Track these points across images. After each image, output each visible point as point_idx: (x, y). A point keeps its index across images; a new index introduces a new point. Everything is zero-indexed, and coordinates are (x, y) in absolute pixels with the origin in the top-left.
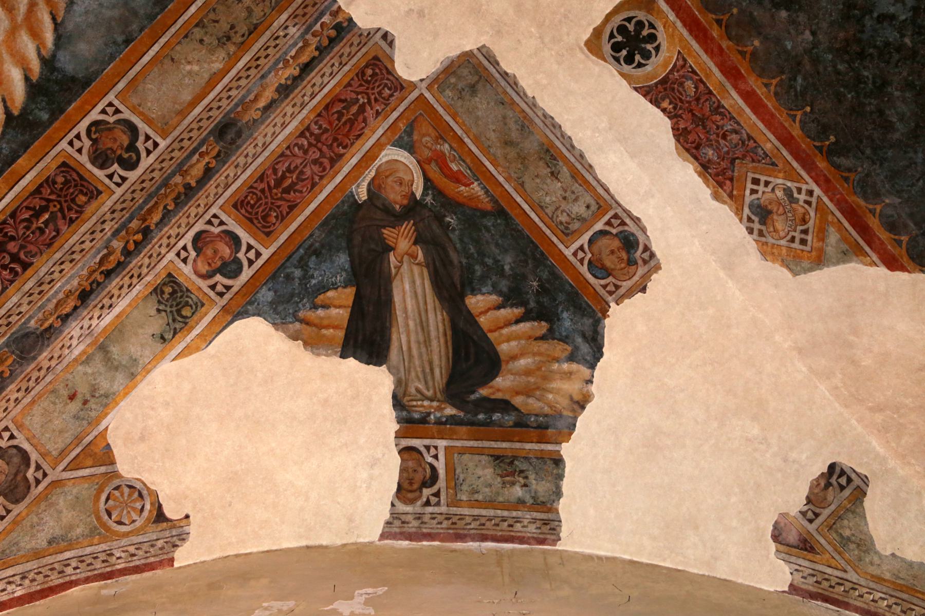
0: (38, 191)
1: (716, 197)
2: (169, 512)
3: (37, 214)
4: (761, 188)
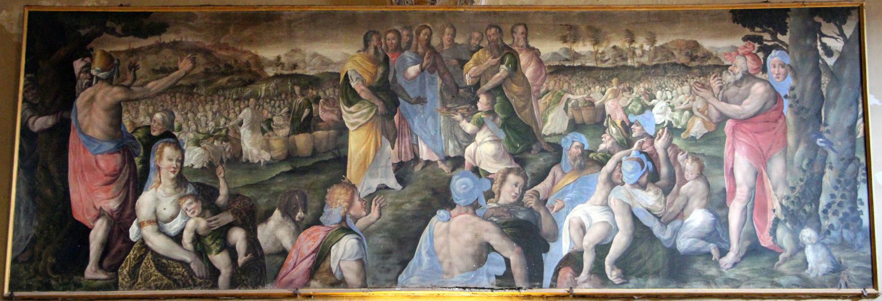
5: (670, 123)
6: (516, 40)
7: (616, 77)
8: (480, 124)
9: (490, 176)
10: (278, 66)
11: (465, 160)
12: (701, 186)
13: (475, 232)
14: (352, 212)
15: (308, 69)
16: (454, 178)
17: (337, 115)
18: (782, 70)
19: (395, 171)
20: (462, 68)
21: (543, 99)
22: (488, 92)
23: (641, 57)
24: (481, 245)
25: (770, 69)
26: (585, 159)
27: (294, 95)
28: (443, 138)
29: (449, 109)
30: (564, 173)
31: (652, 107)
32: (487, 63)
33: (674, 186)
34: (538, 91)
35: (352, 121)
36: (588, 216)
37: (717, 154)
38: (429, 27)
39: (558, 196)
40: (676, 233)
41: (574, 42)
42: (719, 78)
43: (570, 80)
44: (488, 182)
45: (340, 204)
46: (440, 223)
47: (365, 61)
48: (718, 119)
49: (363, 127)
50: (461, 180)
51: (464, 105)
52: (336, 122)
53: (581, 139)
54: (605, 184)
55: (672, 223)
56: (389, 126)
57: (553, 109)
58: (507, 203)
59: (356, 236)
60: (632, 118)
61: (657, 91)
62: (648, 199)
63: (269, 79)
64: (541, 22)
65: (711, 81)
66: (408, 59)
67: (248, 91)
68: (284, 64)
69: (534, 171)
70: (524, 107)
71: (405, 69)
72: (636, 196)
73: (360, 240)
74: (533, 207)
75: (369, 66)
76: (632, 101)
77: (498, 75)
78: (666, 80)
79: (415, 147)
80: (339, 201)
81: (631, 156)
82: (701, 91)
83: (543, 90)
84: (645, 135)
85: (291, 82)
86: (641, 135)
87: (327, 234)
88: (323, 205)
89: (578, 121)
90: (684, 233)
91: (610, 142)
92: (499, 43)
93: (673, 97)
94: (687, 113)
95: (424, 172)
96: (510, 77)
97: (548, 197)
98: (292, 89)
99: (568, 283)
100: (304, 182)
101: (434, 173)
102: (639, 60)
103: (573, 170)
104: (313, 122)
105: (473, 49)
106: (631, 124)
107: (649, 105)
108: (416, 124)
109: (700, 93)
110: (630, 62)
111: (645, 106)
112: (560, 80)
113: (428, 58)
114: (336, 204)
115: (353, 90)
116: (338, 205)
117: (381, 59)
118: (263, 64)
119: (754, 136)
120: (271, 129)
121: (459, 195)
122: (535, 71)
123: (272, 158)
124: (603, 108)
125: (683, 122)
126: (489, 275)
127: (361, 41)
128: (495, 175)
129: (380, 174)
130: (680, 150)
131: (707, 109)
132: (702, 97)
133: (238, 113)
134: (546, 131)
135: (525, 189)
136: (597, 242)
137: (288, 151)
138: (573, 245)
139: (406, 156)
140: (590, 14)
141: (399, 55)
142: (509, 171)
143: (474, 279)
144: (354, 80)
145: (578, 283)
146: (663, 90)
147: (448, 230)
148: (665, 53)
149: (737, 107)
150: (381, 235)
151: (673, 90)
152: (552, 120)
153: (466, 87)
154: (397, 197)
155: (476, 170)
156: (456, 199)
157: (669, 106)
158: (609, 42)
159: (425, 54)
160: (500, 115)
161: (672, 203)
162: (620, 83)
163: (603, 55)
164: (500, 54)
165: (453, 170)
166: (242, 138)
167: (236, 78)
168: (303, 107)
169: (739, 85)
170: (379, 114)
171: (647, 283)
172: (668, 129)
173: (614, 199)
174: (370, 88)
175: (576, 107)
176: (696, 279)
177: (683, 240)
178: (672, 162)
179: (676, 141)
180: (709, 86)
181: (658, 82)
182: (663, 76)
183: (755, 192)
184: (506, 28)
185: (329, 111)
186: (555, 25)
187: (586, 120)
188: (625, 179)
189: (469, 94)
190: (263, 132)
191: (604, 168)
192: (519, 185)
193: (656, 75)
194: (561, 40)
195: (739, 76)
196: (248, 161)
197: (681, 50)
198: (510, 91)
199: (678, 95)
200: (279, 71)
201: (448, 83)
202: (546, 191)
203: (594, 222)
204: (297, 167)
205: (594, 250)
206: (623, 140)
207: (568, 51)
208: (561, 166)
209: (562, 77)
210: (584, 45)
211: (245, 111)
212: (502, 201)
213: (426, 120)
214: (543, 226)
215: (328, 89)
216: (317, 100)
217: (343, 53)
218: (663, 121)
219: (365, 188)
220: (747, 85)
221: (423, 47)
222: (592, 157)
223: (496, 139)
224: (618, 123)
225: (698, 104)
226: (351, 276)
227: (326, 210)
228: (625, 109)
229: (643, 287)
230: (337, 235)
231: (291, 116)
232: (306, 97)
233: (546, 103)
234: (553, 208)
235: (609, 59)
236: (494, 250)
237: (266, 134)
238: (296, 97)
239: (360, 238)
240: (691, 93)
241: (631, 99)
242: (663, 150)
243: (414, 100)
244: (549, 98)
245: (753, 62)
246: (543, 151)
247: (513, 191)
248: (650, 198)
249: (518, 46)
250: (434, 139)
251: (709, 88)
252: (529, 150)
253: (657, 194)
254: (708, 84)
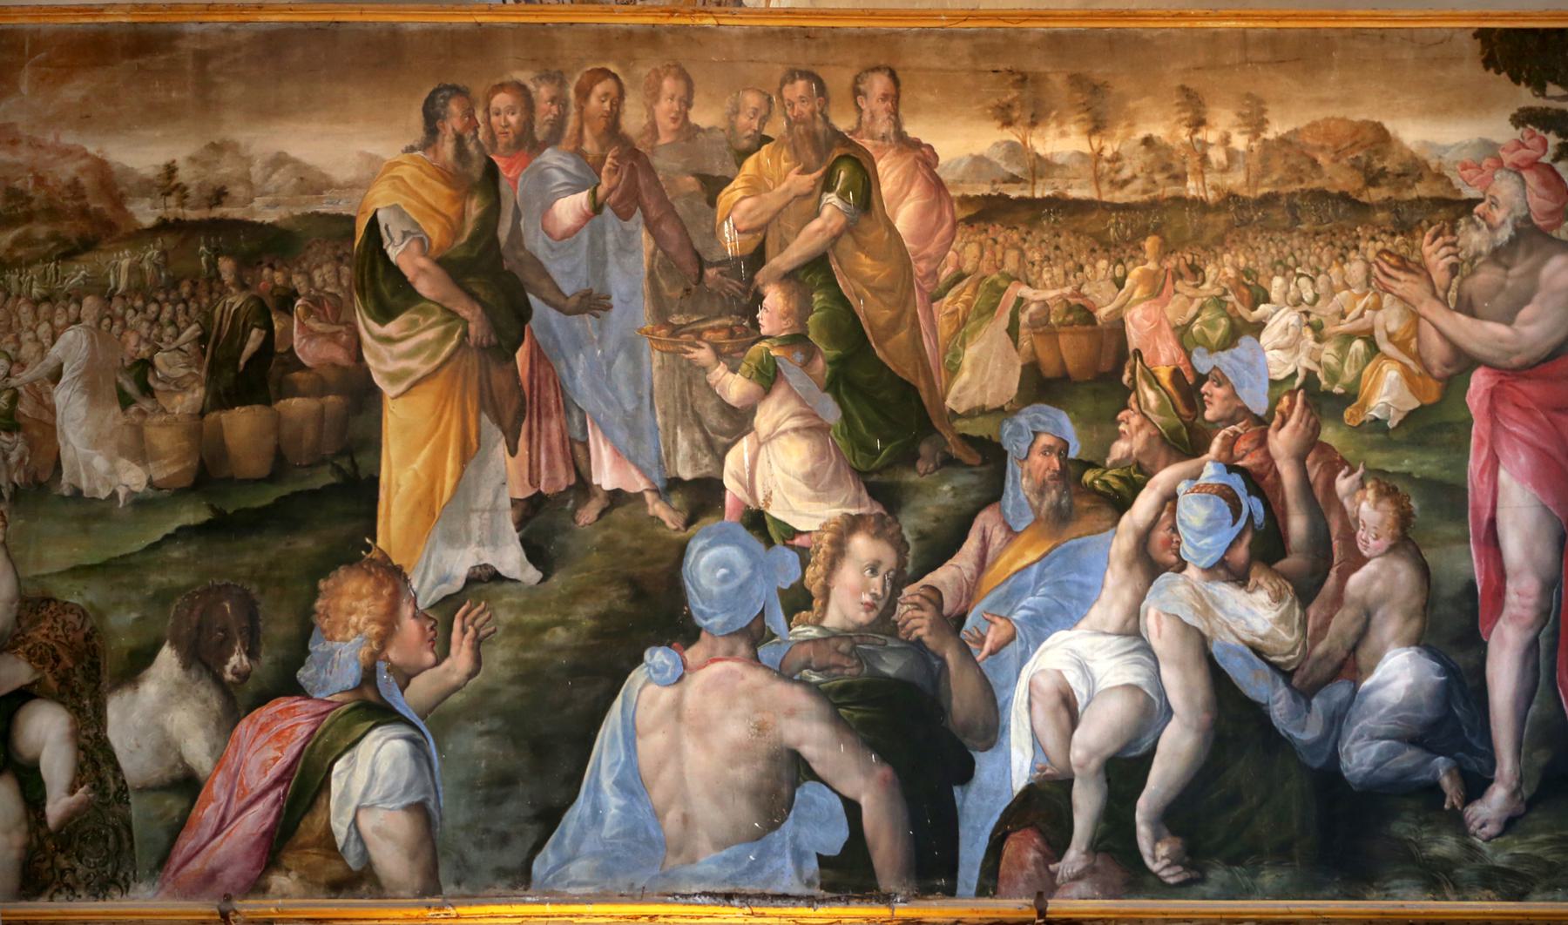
5: (1310, 375)
6: (866, 117)
7: (1155, 232)
8: (768, 378)
9: (797, 541)
10: (169, 194)
11: (723, 489)
12: (1403, 573)
13: (758, 717)
14: (393, 654)
15: (258, 203)
16: (695, 546)
17: (346, 347)
19: (520, 525)
20: (712, 203)
21: (948, 298)
22: (789, 278)
23: (1225, 170)
24: (774, 758)
26: (1073, 488)
27: (217, 287)
28: (659, 420)
29: (675, 331)
30: (1011, 533)
31: (1258, 327)
32: (784, 186)
33: (1327, 574)
34: (934, 274)
35: (393, 366)
36: (1083, 668)
37: (1447, 475)
38: (615, 77)
39: (996, 603)
40: (1337, 720)
41: (1033, 124)
42: (1448, 239)
43: (1025, 240)
44: (792, 557)
45: (356, 627)
46: (652, 688)
47: (429, 180)
48: (1447, 366)
49: (424, 386)
50: (715, 552)
51: (719, 316)
52: (344, 369)
53: (1058, 426)
54: (1129, 566)
55: (1324, 691)
56: (499, 379)
57: (980, 327)
58: (850, 626)
59: (405, 730)
60: (1203, 363)
61: (1271, 279)
62: (1253, 614)
63: (141, 236)
64: (936, 62)
65: (1427, 250)
66: (555, 173)
67: (77, 273)
68: (185, 188)
69: (928, 525)
70: (893, 326)
71: (547, 207)
72: (1220, 605)
73: (417, 744)
74: (926, 639)
75: (438, 194)
76: (1202, 307)
77: (816, 224)
78: (1296, 243)
79: (578, 447)
80: (354, 619)
81: (1202, 480)
82: (1398, 280)
83: (946, 273)
84: (1241, 415)
85: (208, 246)
86: (1229, 413)
87: (318, 724)
88: (306, 629)
89: (1050, 369)
90: (1364, 722)
91: (1142, 435)
92: (820, 127)
93: (1317, 297)
94: (1358, 345)
95: (606, 526)
96: (850, 229)
97: (967, 606)
98: (213, 264)
99: (1029, 880)
100: (248, 557)
101: (636, 529)
102: (1219, 182)
103: (1037, 521)
104: (274, 369)
105: (745, 143)
106: (1201, 379)
107: (1250, 320)
108: (580, 374)
109: (1394, 283)
110: (1192, 188)
111: (1238, 322)
112: (995, 241)
113: (615, 170)
114: (346, 627)
115: (394, 271)
116: (352, 632)
117: (476, 170)
118: (123, 189)
119: (1549, 419)
120: (147, 391)
121: (707, 598)
122: (924, 213)
123: (150, 483)
124: (1118, 328)
125: (1349, 373)
126: (799, 857)
127: (416, 119)
128: (814, 537)
129: (476, 533)
130: (1344, 462)
131: (1417, 334)
132: (1401, 299)
133: (47, 342)
134: (956, 399)
135: (898, 581)
136: (1111, 750)
137: (201, 461)
138: (1042, 760)
139: (553, 479)
140: (1078, 36)
141: (529, 158)
142: (853, 524)
143: (754, 868)
144: (397, 240)
145: (1058, 881)
146: (1290, 273)
147: (677, 708)
148: (1292, 161)
149: (1501, 330)
150: (479, 727)
151: (1318, 273)
152: (974, 366)
153: (725, 262)
154: (525, 608)
155: (756, 521)
156: (701, 613)
157: (1308, 324)
158: (1131, 125)
159: (604, 158)
160: (822, 347)
161: (1324, 626)
162: (1166, 250)
163: (1118, 165)
164: (821, 160)
165: (689, 523)
166: (59, 419)
167: (41, 230)
168: (245, 324)
169: (1504, 260)
170: (472, 343)
171: (1259, 880)
172: (1306, 395)
173: (1158, 617)
174: (443, 262)
175: (1041, 323)
176: (1398, 869)
177: (1359, 744)
178: (1320, 499)
179: (1329, 435)
180: (1419, 264)
181: (1273, 251)
182: (1289, 230)
183: (1559, 593)
184: (839, 79)
185: (323, 334)
186: (976, 72)
187: (1072, 366)
188: (1187, 551)
189: (733, 285)
190: (125, 401)
191: (1126, 518)
192: (882, 570)
193: (1267, 227)
194: (995, 118)
195: (1504, 234)
196: (77, 493)
197: (1337, 152)
198: (853, 275)
199: (1333, 291)
200: (173, 209)
201: (672, 249)
202: (960, 589)
203: (1102, 685)
204: (230, 511)
205: (1102, 777)
206: (1178, 429)
207: (1014, 150)
208: (1002, 513)
209: (999, 232)
210: (1063, 134)
211: (69, 334)
212: (833, 619)
213: (610, 364)
214: (955, 704)
215: (319, 266)
216: (286, 301)
217: (362, 154)
218: (1290, 370)
219: (431, 577)
220: (1530, 262)
221: (598, 138)
222: (1092, 483)
223: (816, 422)
224: (1164, 374)
225: (1390, 319)
226: (391, 859)
227: (317, 647)
228: (1182, 333)
229: (1247, 893)
230: (348, 728)
231: (209, 351)
232: (255, 293)
233: (955, 312)
234: (981, 641)
235: (1134, 177)
236: (814, 777)
237: (133, 409)
238: (224, 292)
239: (419, 737)
240: (1369, 285)
241: (1198, 302)
242: (1293, 462)
243: (573, 303)
244: (964, 297)
245: (1543, 191)
246: (949, 462)
247: (865, 588)
248: (1261, 611)
249: (872, 137)
250: (633, 427)
251: (1419, 269)
252: (909, 458)
253: (1278, 598)
254: (1415, 258)
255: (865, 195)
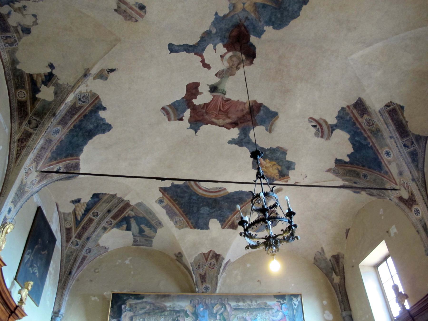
0: (87, 221)
1: (171, 220)
2: (107, 247)
3: (87, 223)
4: (176, 219)
18: (285, 309)
20: (213, 308)
22: (220, 315)
23: (254, 306)
25: (283, 309)
29: (210, 319)
31: (257, 318)
63: (168, 311)
67: (163, 314)
75: (191, 308)
77: (221, 310)
83: (232, 314)
94: (265, 319)
110: (251, 307)
117: (194, 306)
124: (246, 319)
162: (250, 312)
167: (160, 310)
184: (223, 299)
195: (276, 311)
209: (236, 311)
216: (179, 316)
225: (267, 317)
255: (225, 308)
